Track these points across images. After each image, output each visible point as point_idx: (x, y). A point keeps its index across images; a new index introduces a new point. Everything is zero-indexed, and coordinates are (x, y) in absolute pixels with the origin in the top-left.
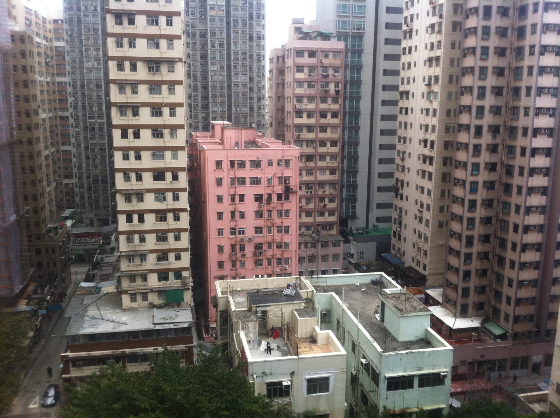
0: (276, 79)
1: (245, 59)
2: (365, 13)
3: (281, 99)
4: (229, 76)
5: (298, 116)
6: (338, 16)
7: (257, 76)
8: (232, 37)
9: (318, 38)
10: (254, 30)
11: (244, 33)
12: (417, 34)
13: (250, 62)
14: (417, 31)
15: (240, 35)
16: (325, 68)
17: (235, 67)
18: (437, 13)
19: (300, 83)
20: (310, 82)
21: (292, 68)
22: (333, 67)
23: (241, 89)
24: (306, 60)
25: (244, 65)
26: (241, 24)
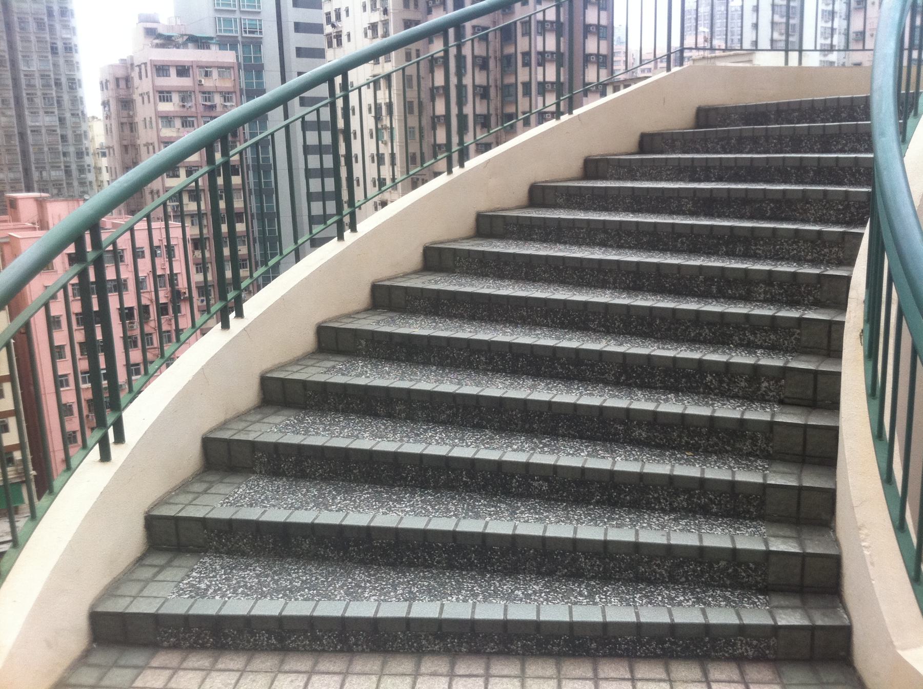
0: (118, 116)
1: (47, 86)
2: (259, 7)
3: (130, 149)
4: (20, 117)
5: (171, 174)
6: (216, 10)
7: (73, 115)
8: (20, 48)
9: (190, 45)
10: (58, 33)
11: (40, 40)
12: (349, 40)
13: (57, 92)
14: (349, 35)
15: (34, 46)
16: (207, 94)
17: (31, 100)
18: (378, 6)
19: (167, 119)
20: (186, 117)
21: (151, 95)
22: (221, 92)
23: (45, 138)
24: (173, 81)
25: (45, 96)
26: (35, 25)
